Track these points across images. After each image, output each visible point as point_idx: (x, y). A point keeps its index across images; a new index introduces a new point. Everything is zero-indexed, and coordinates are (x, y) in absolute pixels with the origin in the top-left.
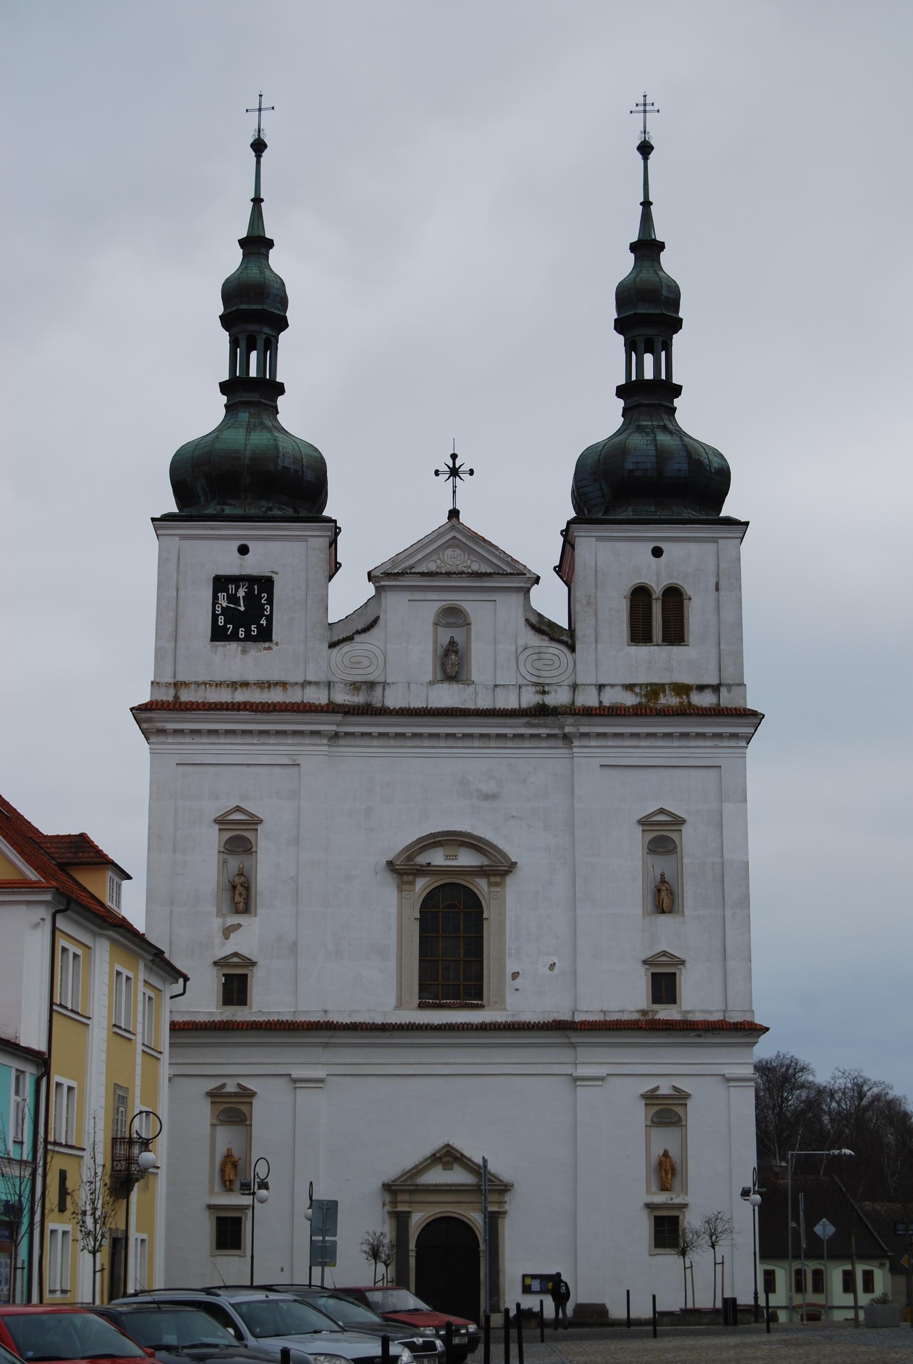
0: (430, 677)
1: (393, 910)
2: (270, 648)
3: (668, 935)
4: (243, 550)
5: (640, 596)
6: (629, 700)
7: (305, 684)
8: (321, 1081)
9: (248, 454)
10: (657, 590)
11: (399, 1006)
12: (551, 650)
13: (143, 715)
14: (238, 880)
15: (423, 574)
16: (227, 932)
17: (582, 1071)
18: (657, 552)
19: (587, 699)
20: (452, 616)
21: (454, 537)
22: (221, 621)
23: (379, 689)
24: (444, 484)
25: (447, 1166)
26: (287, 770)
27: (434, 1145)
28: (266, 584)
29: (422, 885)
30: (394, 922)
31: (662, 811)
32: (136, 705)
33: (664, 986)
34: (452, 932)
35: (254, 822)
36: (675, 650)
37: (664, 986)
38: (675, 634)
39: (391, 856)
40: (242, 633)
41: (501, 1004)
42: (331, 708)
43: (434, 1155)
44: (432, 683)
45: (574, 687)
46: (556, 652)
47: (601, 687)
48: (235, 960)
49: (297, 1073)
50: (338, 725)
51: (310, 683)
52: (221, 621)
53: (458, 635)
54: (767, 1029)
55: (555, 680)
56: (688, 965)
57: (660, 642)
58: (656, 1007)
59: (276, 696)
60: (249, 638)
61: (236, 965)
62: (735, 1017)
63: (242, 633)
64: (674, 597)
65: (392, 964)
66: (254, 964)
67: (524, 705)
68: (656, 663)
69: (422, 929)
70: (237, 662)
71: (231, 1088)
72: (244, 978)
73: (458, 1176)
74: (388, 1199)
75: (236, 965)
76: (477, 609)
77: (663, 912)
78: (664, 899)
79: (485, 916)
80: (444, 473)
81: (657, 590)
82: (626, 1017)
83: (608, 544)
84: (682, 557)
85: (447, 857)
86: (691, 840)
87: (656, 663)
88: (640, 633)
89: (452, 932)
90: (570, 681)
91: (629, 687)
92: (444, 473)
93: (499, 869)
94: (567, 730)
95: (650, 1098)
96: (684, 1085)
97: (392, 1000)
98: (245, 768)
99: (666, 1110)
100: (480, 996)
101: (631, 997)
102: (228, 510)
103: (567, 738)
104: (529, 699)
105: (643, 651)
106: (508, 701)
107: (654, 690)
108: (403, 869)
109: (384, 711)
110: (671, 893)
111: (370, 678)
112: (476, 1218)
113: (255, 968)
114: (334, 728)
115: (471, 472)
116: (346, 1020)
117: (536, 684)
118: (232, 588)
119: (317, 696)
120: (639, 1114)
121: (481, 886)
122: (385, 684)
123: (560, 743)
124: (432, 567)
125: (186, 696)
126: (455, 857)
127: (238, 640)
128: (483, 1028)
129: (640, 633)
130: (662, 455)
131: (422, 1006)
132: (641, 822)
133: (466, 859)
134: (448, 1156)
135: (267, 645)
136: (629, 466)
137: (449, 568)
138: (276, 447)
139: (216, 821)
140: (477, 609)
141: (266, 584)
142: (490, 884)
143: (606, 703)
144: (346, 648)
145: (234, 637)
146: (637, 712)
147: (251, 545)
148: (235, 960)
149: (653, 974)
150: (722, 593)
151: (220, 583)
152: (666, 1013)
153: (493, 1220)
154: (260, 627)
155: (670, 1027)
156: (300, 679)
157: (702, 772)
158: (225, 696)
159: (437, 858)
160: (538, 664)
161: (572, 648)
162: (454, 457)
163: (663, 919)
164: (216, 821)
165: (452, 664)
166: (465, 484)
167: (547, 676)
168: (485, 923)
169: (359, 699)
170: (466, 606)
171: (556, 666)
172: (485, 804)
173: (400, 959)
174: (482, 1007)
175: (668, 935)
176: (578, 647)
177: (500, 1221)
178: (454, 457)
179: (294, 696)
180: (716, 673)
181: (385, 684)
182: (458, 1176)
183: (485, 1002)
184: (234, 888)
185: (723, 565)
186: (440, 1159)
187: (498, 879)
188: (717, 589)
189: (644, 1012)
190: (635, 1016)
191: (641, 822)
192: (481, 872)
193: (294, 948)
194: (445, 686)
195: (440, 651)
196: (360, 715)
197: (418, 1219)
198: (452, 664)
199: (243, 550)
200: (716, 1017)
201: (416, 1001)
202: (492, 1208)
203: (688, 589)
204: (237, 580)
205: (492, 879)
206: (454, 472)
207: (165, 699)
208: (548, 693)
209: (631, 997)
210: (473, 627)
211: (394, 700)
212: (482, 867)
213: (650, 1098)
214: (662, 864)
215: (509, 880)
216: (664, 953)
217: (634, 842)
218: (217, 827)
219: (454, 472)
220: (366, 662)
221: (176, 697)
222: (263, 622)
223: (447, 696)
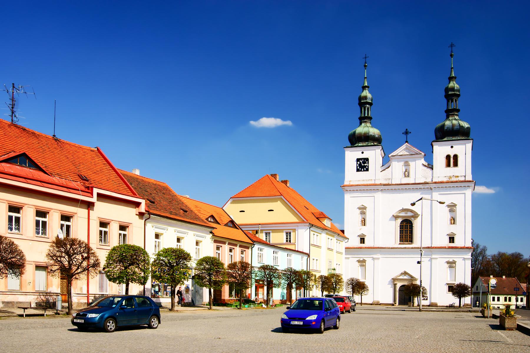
4: (363, 153)
5: (448, 157)
16: (360, 229)
18: (452, 147)
24: (405, 136)
27: (402, 271)
28: (367, 159)
33: (452, 239)
34: (407, 230)
35: (365, 208)
36: (456, 168)
37: (452, 239)
42: (381, 185)
49: (375, 256)
60: (364, 171)
64: (456, 157)
68: (452, 171)
71: (361, 259)
89: (407, 230)
93: (416, 216)
95: (448, 262)
96: (454, 259)
100: (412, 241)
102: (359, 145)
103: (431, 189)
105: (448, 168)
107: (450, 177)
110: (454, 220)
133: (410, 214)
134: (405, 273)
136: (445, 128)
141: (367, 159)
144: (383, 172)
145: (361, 171)
151: (358, 160)
155: (452, 248)
159: (403, 214)
161: (432, 168)
165: (407, 174)
175: (453, 229)
192: (412, 216)
195: (404, 170)
197: (399, 285)
198: (407, 174)
199: (363, 153)
201: (398, 242)
204: (361, 159)
209: (446, 242)
214: (453, 214)
219: (406, 133)
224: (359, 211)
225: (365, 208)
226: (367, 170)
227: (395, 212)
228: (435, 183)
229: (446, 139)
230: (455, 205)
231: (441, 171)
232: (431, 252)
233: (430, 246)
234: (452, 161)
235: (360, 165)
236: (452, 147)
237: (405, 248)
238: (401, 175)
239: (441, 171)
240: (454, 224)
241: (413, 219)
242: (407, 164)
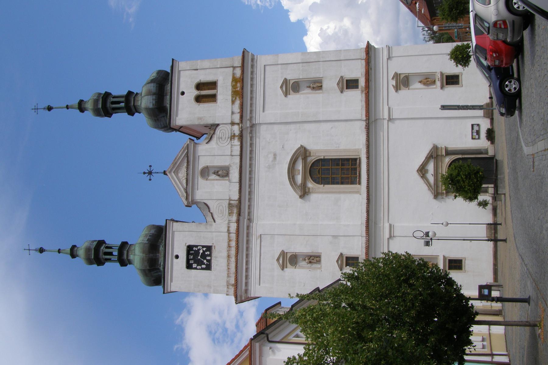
0: (227, 182)
1: (320, 196)
2: (215, 247)
3: (330, 84)
5: (199, 99)
6: (238, 102)
7: (229, 232)
8: (390, 225)
9: (141, 255)
10: (196, 93)
11: (358, 192)
12: (218, 133)
13: (239, 299)
14: (307, 261)
15: (187, 184)
17: (386, 116)
19: (237, 118)
20: (205, 172)
21: (174, 172)
22: (204, 266)
23: (232, 202)
24: (155, 177)
25: (427, 171)
26: (263, 240)
27: (417, 177)
28: (190, 248)
29: (311, 184)
30: (325, 195)
31: (281, 87)
32: (234, 302)
33: (352, 84)
35: (283, 254)
36: (219, 84)
37: (352, 84)
38: (213, 85)
39: (298, 197)
40: (208, 258)
41: (358, 151)
42: (238, 221)
43: (422, 177)
44: (230, 181)
45: (233, 124)
46: (219, 131)
47: (233, 113)
48: (340, 262)
49: (387, 235)
50: (244, 218)
51: (228, 230)
52: (204, 266)
53: (212, 171)
54: (368, 42)
55: (230, 132)
56: (343, 75)
57: (215, 91)
58: (360, 87)
59: (233, 244)
60: (210, 255)
61: (342, 261)
62: (364, 55)
63: (208, 258)
64: (199, 86)
65: (342, 196)
66: (341, 254)
67: (239, 143)
68: (224, 92)
69: (328, 184)
70: (220, 260)
72: (348, 258)
73: (431, 167)
74: (440, 197)
75: (342, 261)
76: (203, 163)
77: (321, 86)
78: (316, 85)
79: (322, 158)
80: (150, 177)
81: (196, 93)
82: (364, 99)
83: (179, 112)
84: (186, 82)
85: (299, 174)
86: (293, 75)
87: (224, 92)
88: (213, 98)
90: (230, 126)
91: (233, 102)
92: (150, 177)
94: (248, 125)
95: (397, 88)
96: (391, 75)
97: (356, 196)
98: (262, 257)
99: (403, 82)
100: (355, 160)
101: (356, 97)
103: (253, 126)
104: (237, 142)
105: (219, 97)
106: (237, 150)
108: (304, 193)
109: (240, 200)
111: (227, 206)
112: (447, 160)
113: (344, 254)
114: (246, 220)
115: (150, 166)
116: (365, 215)
117: (231, 140)
118: (191, 262)
119: (234, 226)
120: (404, 92)
121: (311, 160)
122: (230, 200)
123: (254, 129)
124: (185, 181)
125: (233, 281)
126: (299, 170)
127: (211, 259)
128: (368, 158)
129: (213, 98)
130: (149, 93)
131: (360, 183)
132: (286, 95)
133: (300, 166)
134: (422, 171)
135: (213, 248)
137: (186, 175)
138: (140, 243)
139: (283, 269)
140: (203, 163)
141: (190, 248)
142: (310, 156)
143: (239, 111)
144: (215, 216)
145: (209, 261)
146: (242, 97)
147: (175, 254)
148: (340, 262)
149: (347, 89)
150: (199, 68)
151: (189, 266)
152: (362, 83)
153: (449, 153)
154: (206, 251)
155: (368, 80)
156: (227, 234)
157: (267, 73)
158: (233, 265)
159: (299, 179)
160: (223, 139)
161: (218, 125)
162: (144, 173)
163: (324, 86)
164: (283, 269)
165: (223, 173)
166: (154, 169)
167: (228, 134)
168: (326, 158)
169: (235, 210)
170: (200, 167)
171: (224, 131)
172: (278, 158)
173: (340, 192)
174: (360, 159)
175: (330, 84)
176: (217, 123)
177: (449, 149)
178: (144, 173)
179: (233, 236)
180: (228, 69)
181: (230, 200)
182: (431, 167)
183: (358, 157)
184: (310, 262)
185: (188, 68)
186: (423, 174)
187: (308, 153)
188: (197, 70)
189: (362, 91)
190: (364, 95)
191: (286, 95)
192: (305, 159)
193: (335, 237)
194: (230, 175)
195: (218, 177)
196: (241, 209)
198: (223, 173)
199: (177, 257)
200: (364, 62)
201: (358, 186)
202: (444, 153)
203: (197, 81)
205: (308, 155)
206: (150, 173)
207: (233, 290)
208: (234, 134)
209: (356, 97)
210: (208, 165)
211: (236, 196)
212: (302, 159)
213: (397, 88)
215: (308, 147)
216: (338, 84)
217: (293, 97)
218: (285, 269)
219: (150, 173)
220: (221, 208)
221: (233, 285)
222: (204, 249)
223: (235, 174)
224: (290, 270)
225: (283, 254)
226: (209, 248)
227: (292, 195)
228: (242, 117)
229: (168, 106)
230: (286, 81)
231: (223, 110)
232: (376, 120)
233: (364, 124)
234: (206, 92)
235: (200, 263)
236: (183, 93)
237: (368, 171)
238: (224, 183)
239: (223, 110)
240: (321, 82)
241: (309, 159)
242: (205, 172)
